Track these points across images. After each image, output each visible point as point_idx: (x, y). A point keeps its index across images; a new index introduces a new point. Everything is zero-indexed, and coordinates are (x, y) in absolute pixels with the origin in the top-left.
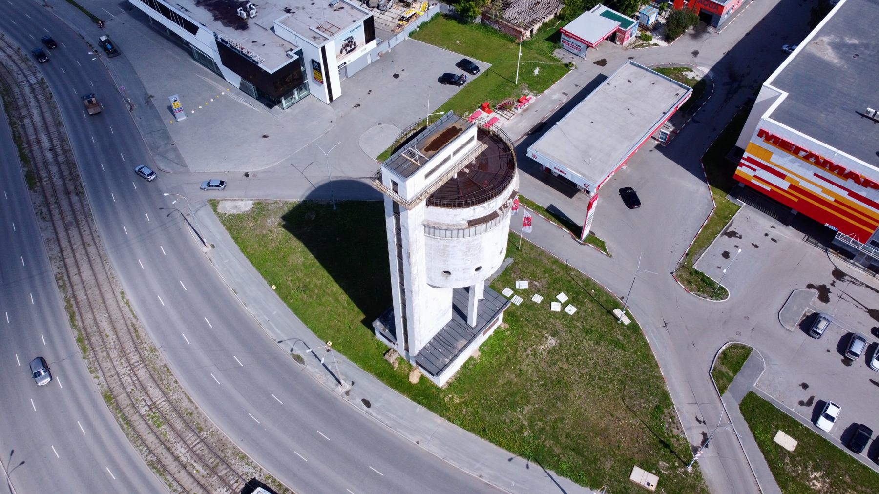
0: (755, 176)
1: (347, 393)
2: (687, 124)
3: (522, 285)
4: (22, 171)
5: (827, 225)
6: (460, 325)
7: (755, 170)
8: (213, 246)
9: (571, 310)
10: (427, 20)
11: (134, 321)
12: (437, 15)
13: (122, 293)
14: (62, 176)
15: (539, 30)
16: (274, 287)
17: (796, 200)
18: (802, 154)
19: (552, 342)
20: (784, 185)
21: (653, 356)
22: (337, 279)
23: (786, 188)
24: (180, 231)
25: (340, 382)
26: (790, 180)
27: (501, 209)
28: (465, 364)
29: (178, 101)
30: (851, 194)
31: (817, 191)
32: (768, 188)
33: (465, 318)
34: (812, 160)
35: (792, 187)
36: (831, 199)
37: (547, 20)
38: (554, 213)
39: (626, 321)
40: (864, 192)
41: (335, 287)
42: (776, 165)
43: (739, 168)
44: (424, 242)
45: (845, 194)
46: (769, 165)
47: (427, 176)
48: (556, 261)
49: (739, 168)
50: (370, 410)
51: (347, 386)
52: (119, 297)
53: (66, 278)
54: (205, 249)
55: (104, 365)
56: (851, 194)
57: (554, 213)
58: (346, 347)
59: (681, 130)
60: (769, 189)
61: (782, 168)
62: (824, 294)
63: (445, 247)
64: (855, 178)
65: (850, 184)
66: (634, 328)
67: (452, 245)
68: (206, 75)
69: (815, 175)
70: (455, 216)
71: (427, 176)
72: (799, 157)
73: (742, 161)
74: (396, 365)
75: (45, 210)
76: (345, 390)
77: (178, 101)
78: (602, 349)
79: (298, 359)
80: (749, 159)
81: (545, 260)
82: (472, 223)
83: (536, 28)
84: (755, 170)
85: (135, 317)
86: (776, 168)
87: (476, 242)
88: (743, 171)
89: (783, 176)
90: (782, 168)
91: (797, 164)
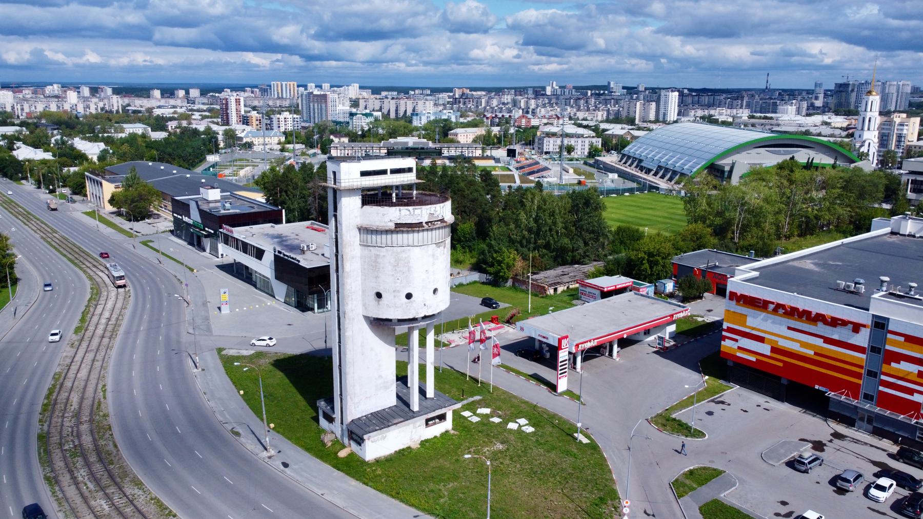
0: (739, 348)
1: (270, 457)
2: (689, 342)
3: (487, 411)
4: (76, 323)
5: (817, 387)
6: (403, 411)
7: (736, 340)
8: (203, 370)
9: (530, 429)
10: (465, 283)
11: (102, 400)
12: (475, 282)
13: (104, 386)
14: (105, 330)
15: (563, 291)
16: (242, 392)
17: (781, 364)
18: (771, 307)
19: (500, 447)
20: (765, 349)
21: (607, 466)
22: (302, 394)
23: (768, 353)
24: (181, 362)
25: (266, 449)
26: (770, 342)
27: (427, 223)
28: (400, 451)
29: (227, 294)
30: (828, 340)
31: (795, 347)
32: (753, 358)
33: (407, 405)
34: (781, 311)
35: (774, 350)
36: (810, 353)
37: (571, 287)
38: (537, 378)
39: (585, 441)
40: (836, 334)
41: (299, 397)
42: (753, 329)
43: (723, 343)
44: (359, 254)
45: (820, 342)
46: (748, 330)
47: (364, 174)
48: (526, 403)
49: (723, 343)
50: (286, 470)
51: (272, 452)
52: (100, 386)
53: (63, 375)
54: (195, 370)
55: (55, 420)
56: (828, 340)
57: (537, 378)
58: (287, 429)
59: (682, 345)
60: (754, 359)
61: (759, 330)
62: (819, 446)
63: (377, 256)
64: (820, 318)
65: (821, 329)
66: (593, 447)
67: (382, 254)
68: (261, 296)
69: (789, 328)
70: (384, 215)
71: (364, 174)
72: (769, 312)
73: (724, 333)
74: (330, 444)
75: (77, 343)
76: (269, 454)
77: (227, 294)
78: (553, 455)
79: (238, 434)
80: (730, 330)
81: (513, 400)
82: (401, 228)
83: (560, 289)
84: (736, 340)
85: (105, 398)
86: (754, 332)
87: (404, 255)
88: (728, 345)
89: (761, 340)
90: (759, 330)
91: (770, 321)
